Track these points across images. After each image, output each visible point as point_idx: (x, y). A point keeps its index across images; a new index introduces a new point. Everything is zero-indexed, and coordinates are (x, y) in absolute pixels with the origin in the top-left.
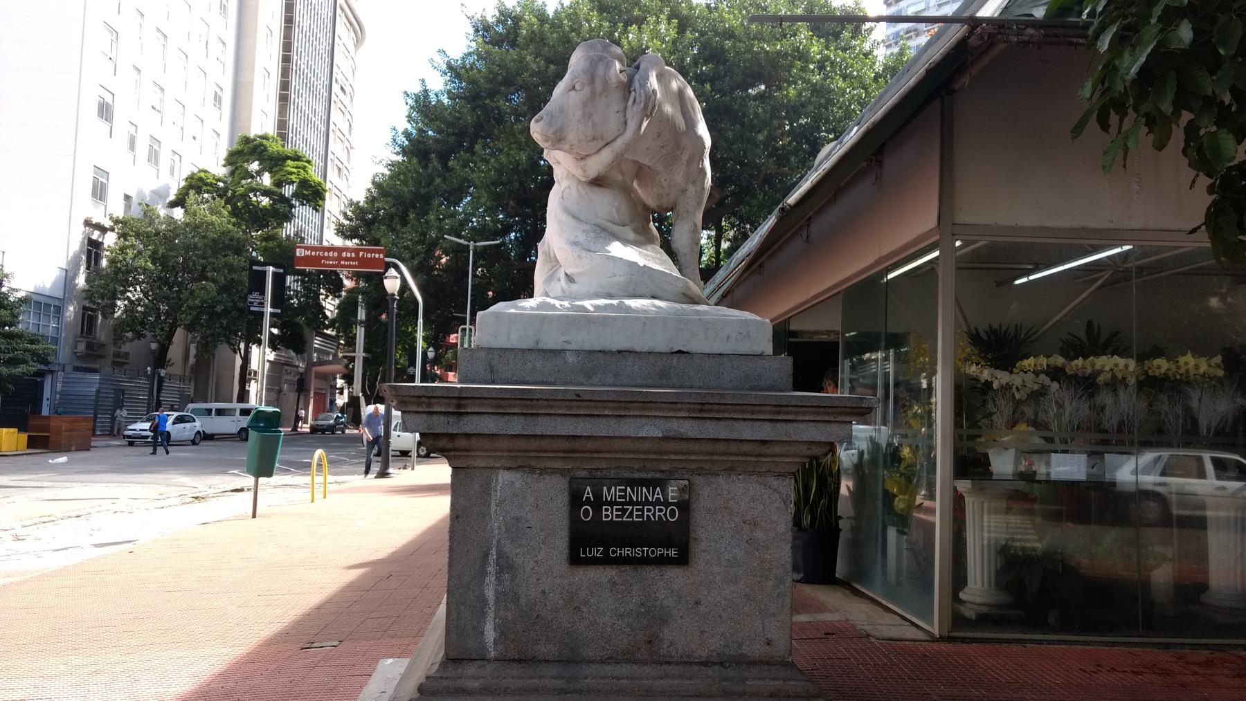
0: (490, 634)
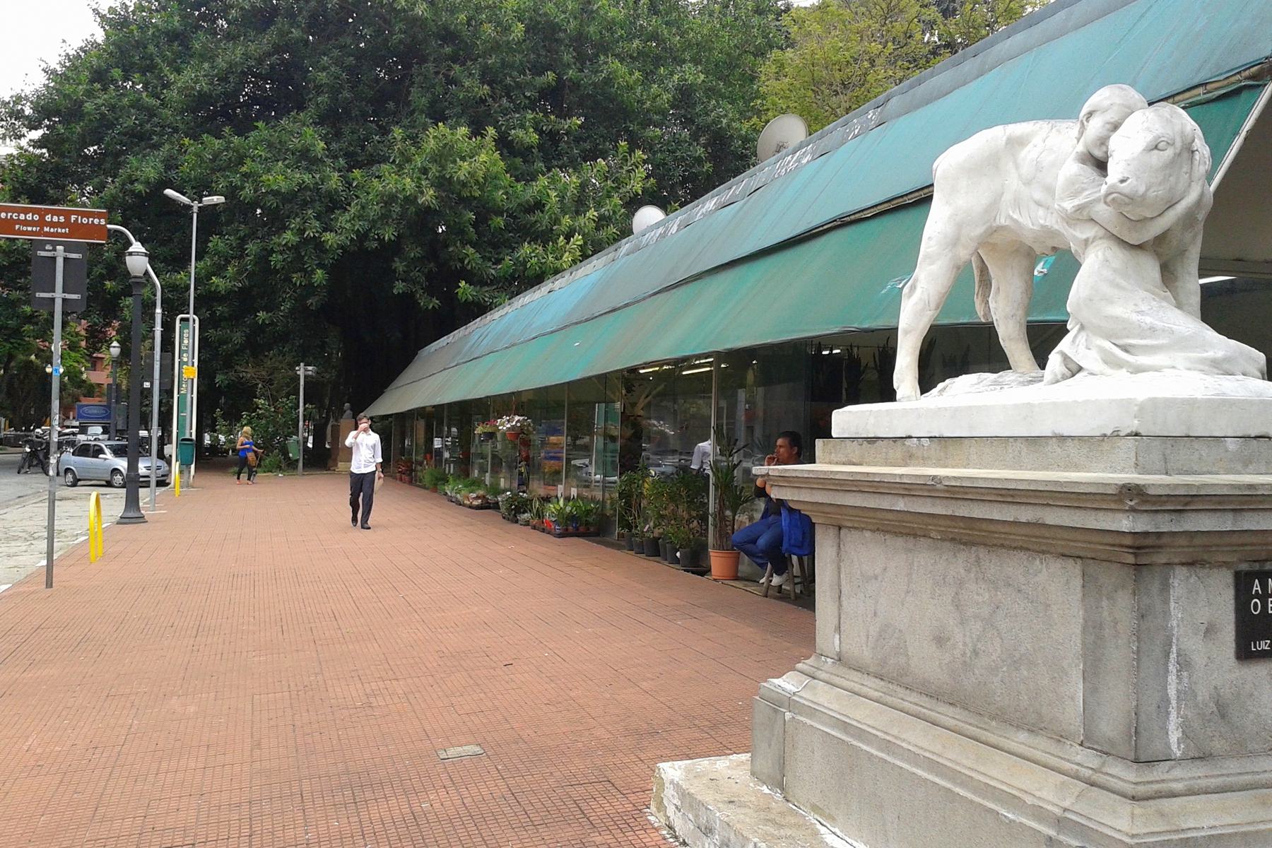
0: (1174, 736)
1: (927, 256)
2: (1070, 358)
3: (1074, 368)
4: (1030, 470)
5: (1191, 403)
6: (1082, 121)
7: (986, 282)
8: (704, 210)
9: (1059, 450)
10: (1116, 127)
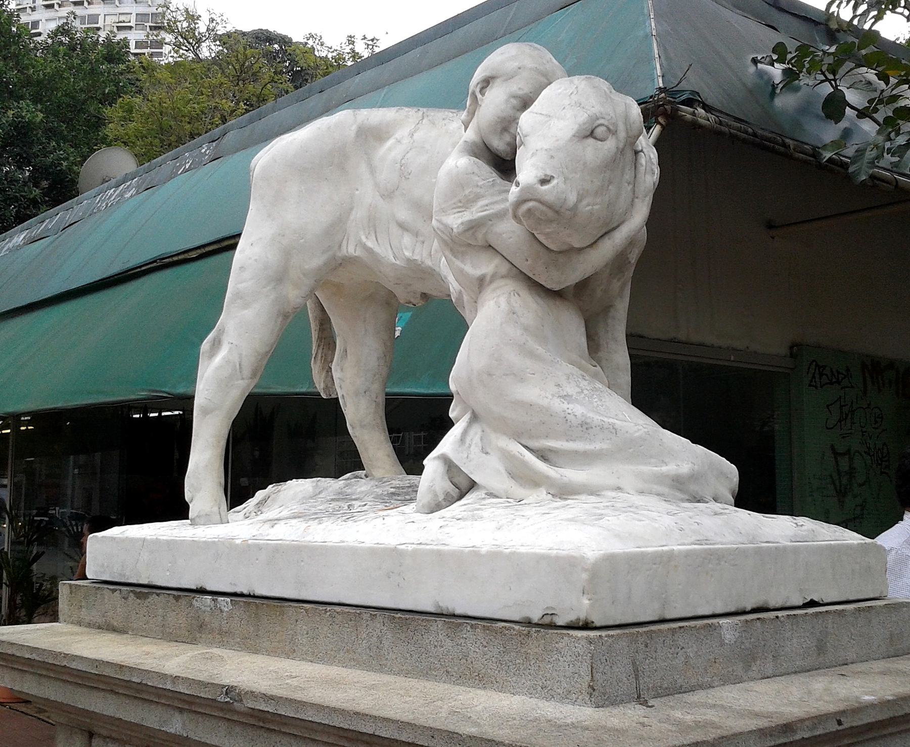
1: (238, 295)
2: (457, 466)
3: (464, 484)
4: (398, 674)
5: (665, 560)
6: (474, 93)
7: (328, 340)
8: (11, 245)
9: (448, 643)
10: (525, 103)
